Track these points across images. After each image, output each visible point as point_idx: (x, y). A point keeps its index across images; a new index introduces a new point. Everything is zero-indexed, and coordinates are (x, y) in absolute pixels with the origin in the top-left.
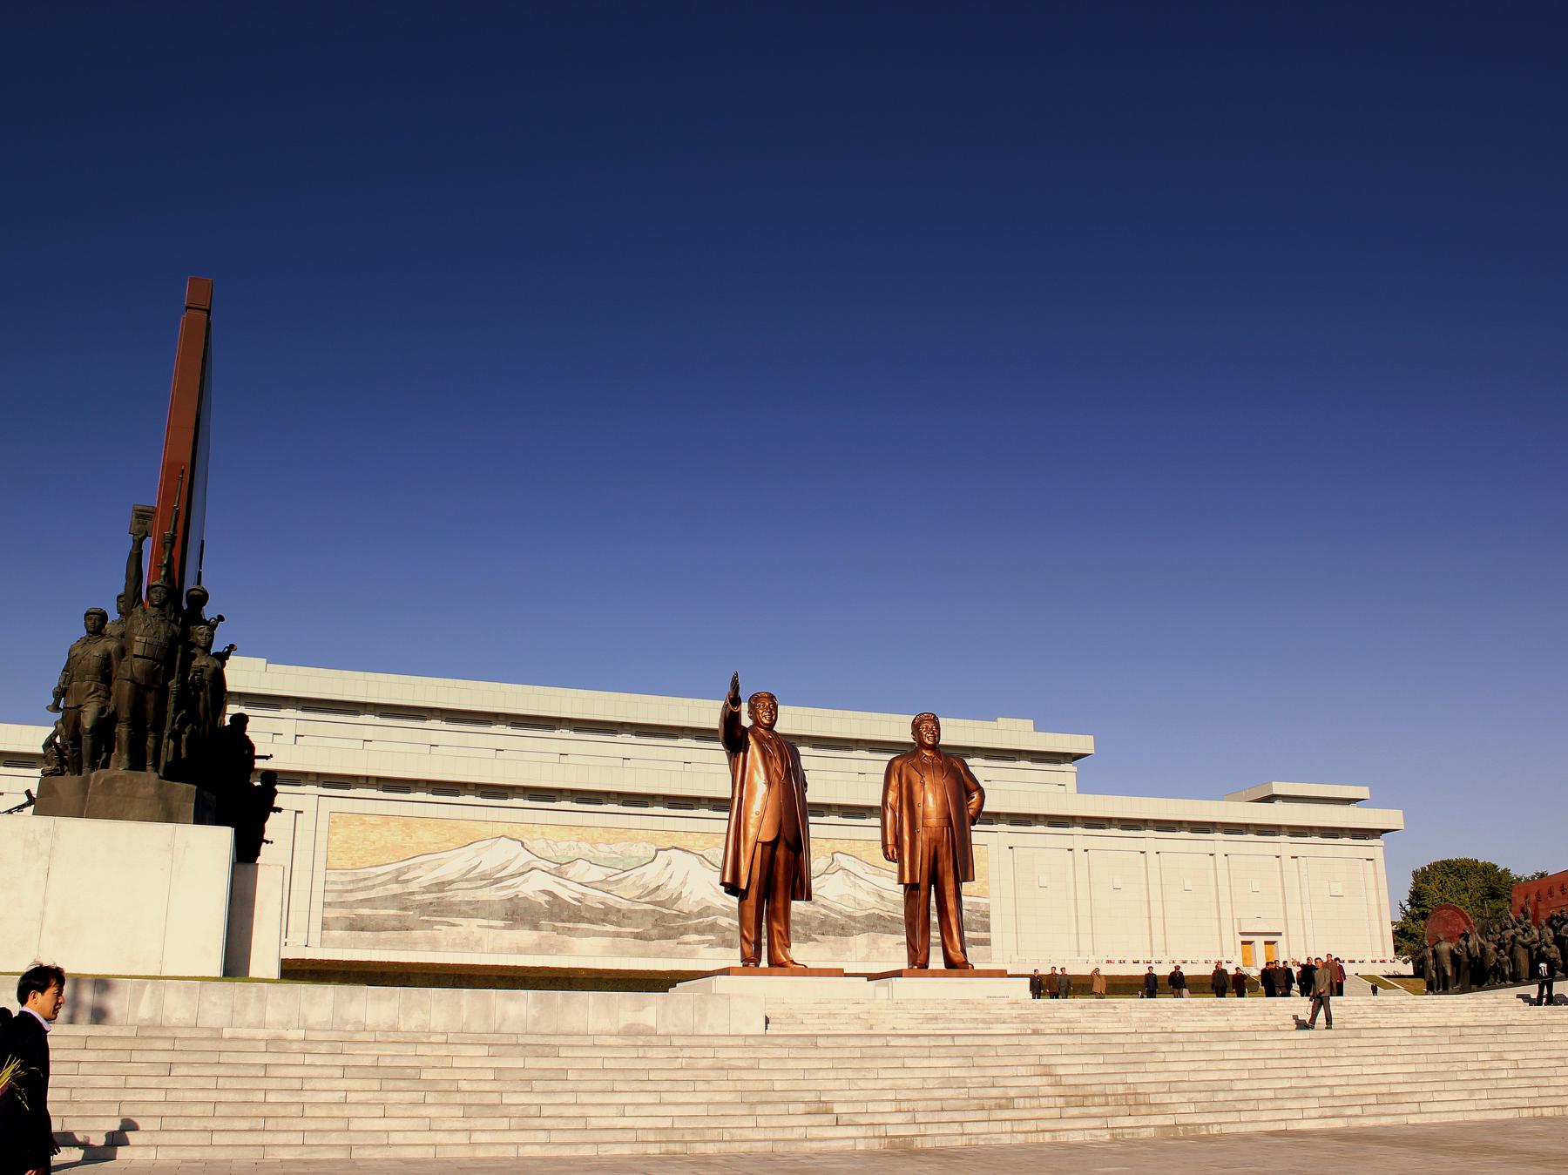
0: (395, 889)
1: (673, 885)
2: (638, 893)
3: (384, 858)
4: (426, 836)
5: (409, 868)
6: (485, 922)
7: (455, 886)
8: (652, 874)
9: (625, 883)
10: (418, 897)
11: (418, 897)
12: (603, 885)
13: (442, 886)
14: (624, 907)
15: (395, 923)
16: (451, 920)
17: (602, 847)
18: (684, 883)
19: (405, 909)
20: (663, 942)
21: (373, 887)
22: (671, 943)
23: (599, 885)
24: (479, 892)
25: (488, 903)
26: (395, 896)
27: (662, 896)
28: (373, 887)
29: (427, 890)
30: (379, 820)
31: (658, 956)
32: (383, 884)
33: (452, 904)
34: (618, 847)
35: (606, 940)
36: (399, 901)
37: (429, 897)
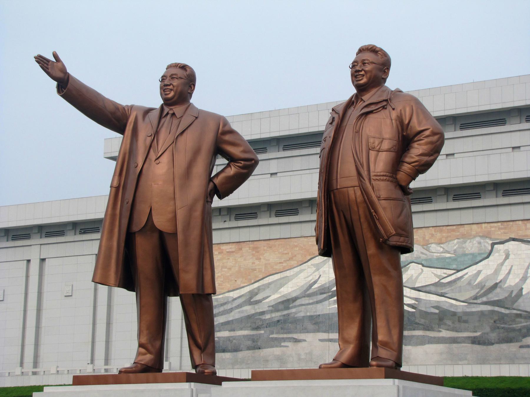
0: (249, 310)
1: (512, 281)
2: (473, 293)
3: (239, 283)
4: (271, 257)
5: (259, 289)
6: (324, 336)
7: (298, 302)
8: (485, 270)
9: (459, 284)
10: (268, 316)
11: (268, 316)
12: (436, 288)
13: (287, 303)
14: (459, 310)
15: (249, 343)
16: (295, 336)
17: (434, 247)
18: (524, 279)
19: (257, 328)
20: (504, 346)
21: (231, 310)
22: (513, 347)
23: (433, 289)
24: (319, 307)
25: (328, 316)
26: (249, 317)
27: (497, 295)
28: (231, 310)
29: (275, 308)
30: (233, 248)
31: (498, 360)
32: (239, 306)
33: (296, 321)
34: (454, 245)
35: (441, 347)
36: (254, 322)
37: (276, 315)
